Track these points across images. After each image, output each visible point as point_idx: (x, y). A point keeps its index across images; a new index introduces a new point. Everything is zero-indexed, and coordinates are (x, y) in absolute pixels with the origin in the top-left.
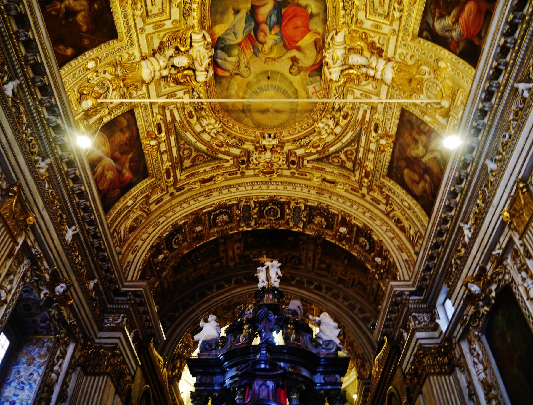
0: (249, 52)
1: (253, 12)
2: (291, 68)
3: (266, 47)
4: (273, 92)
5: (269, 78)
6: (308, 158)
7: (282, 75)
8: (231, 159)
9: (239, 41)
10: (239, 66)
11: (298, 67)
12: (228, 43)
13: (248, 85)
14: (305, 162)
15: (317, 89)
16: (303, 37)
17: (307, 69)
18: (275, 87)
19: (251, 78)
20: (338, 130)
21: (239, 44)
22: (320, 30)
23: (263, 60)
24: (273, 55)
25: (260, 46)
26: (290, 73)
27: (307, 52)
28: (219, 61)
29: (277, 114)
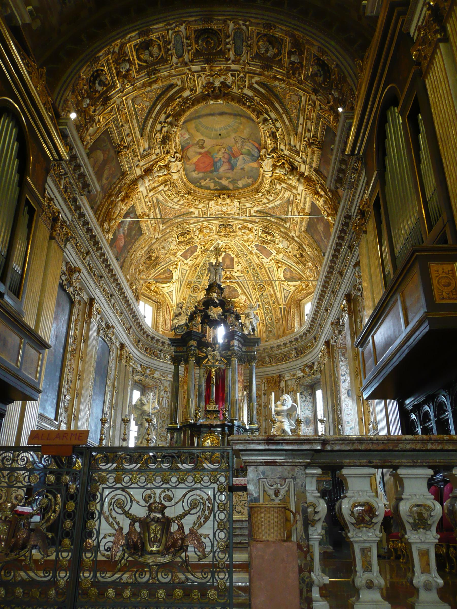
0: (235, 149)
1: (232, 167)
2: (204, 143)
3: (223, 150)
4: (216, 127)
5: (220, 135)
6: (177, 88)
7: (210, 138)
8: (253, 84)
9: (242, 156)
10: (243, 143)
11: (198, 144)
12: (250, 157)
13: (235, 131)
14: (179, 83)
15: (182, 138)
16: (199, 159)
17: (192, 146)
18: (215, 131)
19: (233, 135)
20: (159, 127)
21: (242, 154)
22: (187, 166)
23: (225, 145)
24: (218, 147)
25: (227, 151)
26: (204, 140)
27: (193, 154)
28: (256, 150)
29: (212, 112)
